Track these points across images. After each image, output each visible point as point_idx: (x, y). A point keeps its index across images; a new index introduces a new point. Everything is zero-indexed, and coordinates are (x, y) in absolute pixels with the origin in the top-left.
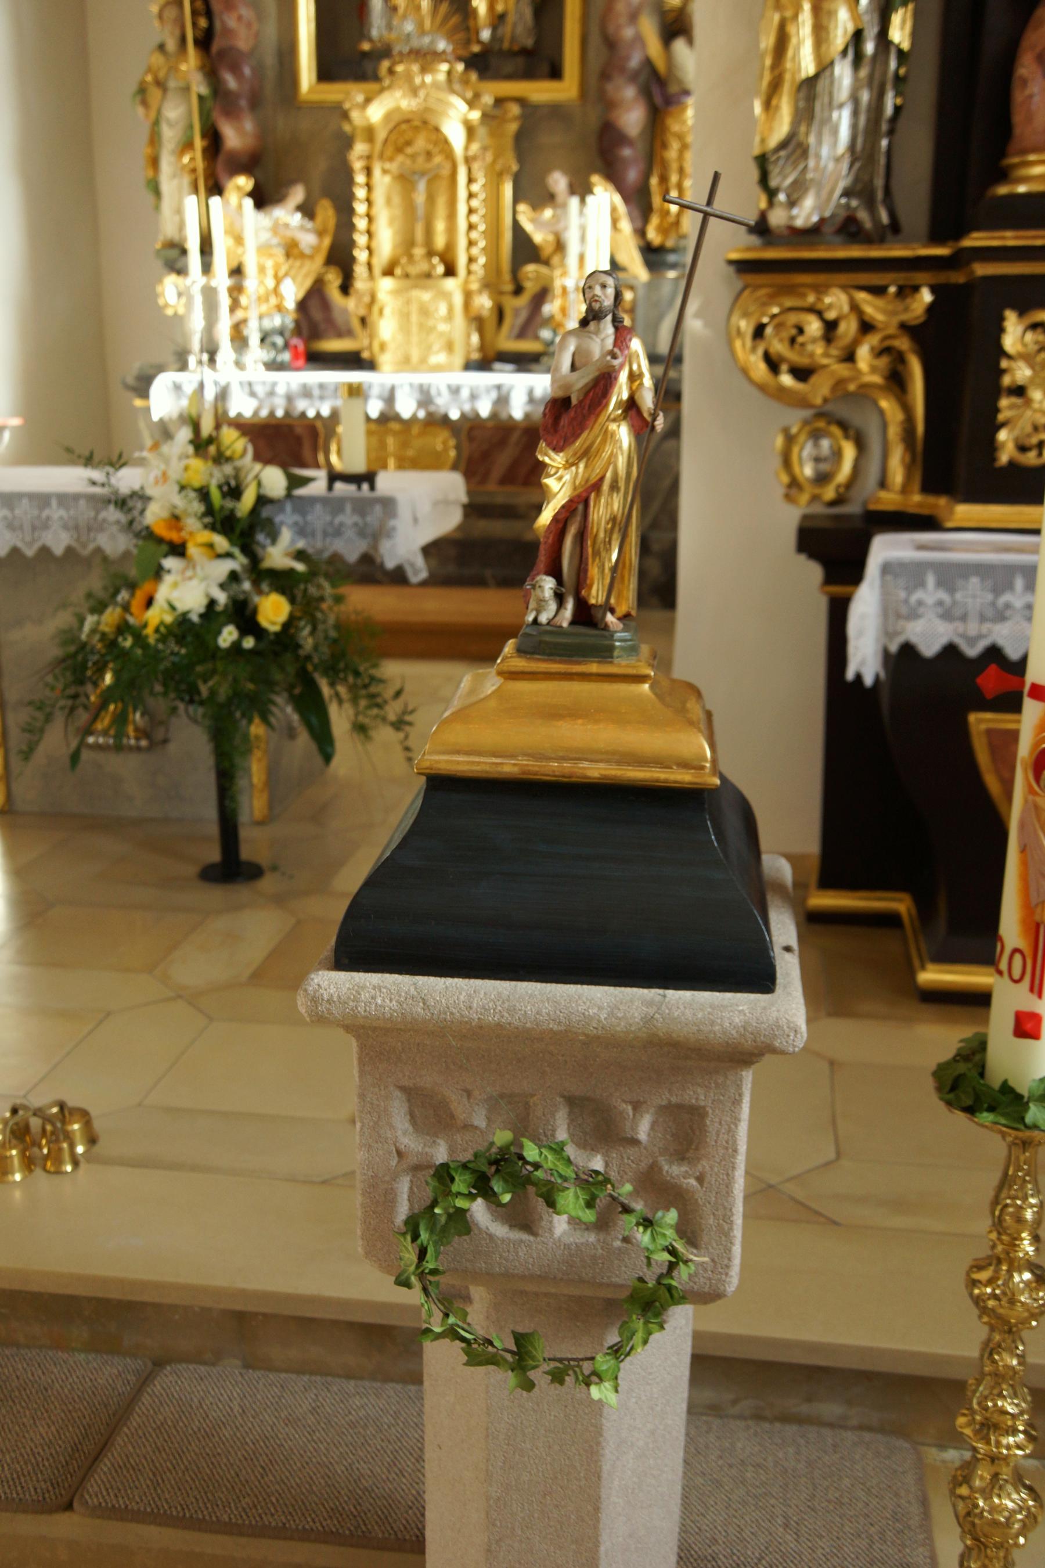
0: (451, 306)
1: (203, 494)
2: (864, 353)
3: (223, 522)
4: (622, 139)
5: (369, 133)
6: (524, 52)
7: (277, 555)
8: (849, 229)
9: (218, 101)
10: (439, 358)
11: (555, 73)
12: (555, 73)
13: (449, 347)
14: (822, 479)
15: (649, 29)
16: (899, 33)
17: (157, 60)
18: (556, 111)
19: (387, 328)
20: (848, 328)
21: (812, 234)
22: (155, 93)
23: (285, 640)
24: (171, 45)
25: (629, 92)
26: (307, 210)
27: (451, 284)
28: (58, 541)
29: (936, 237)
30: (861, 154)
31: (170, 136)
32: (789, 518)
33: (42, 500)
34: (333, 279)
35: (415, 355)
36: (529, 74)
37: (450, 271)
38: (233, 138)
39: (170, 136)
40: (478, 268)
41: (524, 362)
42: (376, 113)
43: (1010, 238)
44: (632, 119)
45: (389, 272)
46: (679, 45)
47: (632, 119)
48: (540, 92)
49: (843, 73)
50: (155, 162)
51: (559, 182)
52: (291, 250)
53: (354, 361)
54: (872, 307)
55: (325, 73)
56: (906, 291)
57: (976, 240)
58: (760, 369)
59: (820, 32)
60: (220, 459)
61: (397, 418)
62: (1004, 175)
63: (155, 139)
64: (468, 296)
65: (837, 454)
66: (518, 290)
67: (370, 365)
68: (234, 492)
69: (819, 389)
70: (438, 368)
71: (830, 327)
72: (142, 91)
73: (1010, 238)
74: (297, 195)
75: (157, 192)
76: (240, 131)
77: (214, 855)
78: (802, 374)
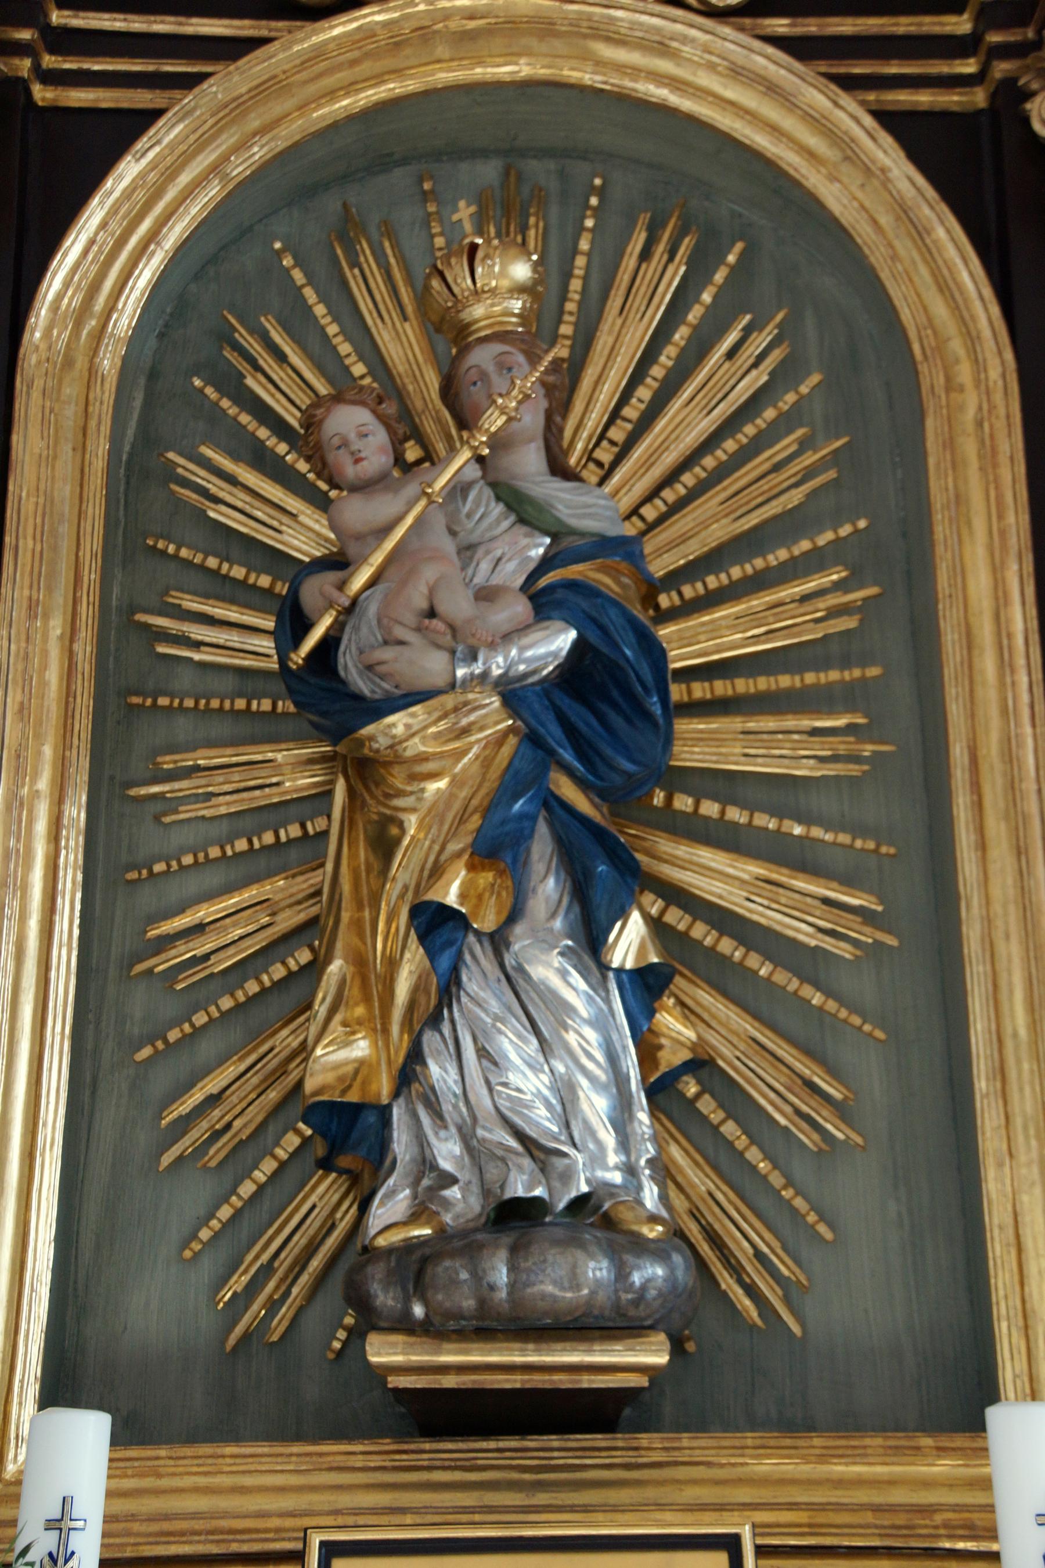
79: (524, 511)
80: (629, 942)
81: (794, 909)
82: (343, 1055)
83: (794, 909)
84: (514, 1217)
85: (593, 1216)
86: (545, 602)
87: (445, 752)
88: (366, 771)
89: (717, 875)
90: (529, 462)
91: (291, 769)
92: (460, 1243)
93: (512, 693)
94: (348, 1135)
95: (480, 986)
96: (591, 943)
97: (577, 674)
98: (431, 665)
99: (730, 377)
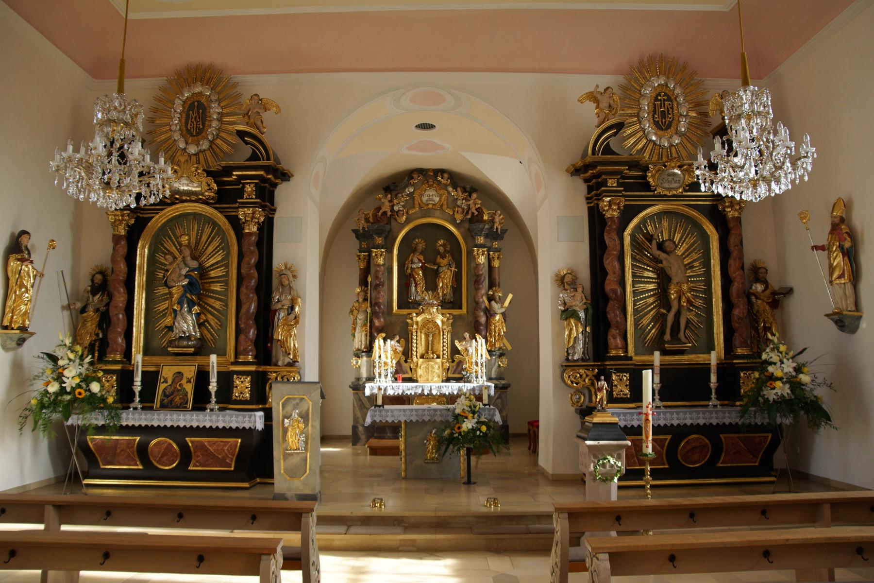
0: (437, 366)
1: (470, 407)
2: (587, 380)
3: (474, 413)
4: (481, 324)
5: (417, 323)
6: (451, 302)
7: (483, 419)
8: (583, 360)
9: (374, 314)
10: (436, 379)
11: (461, 308)
12: (461, 308)
13: (439, 376)
14: (578, 402)
15: (485, 299)
16: (588, 329)
17: (357, 305)
18: (460, 316)
19: (420, 372)
20: (584, 376)
21: (577, 361)
22: (355, 312)
23: (485, 434)
24: (361, 300)
25: (482, 314)
26: (398, 342)
27: (438, 360)
28: (427, 418)
29: (595, 361)
30: (584, 348)
31: (360, 322)
32: (573, 409)
33: (424, 410)
34: (403, 358)
35: (430, 379)
36: (453, 308)
37: (438, 357)
38: (377, 323)
39: (360, 322)
40: (445, 356)
41: (458, 380)
42: (419, 319)
43: (612, 363)
44: (483, 320)
45: (422, 357)
46: (493, 303)
47: (483, 320)
48: (456, 312)
49: (580, 335)
50: (355, 329)
51: (467, 335)
52: (395, 351)
53: (410, 380)
54: (588, 373)
55: (399, 307)
56: (593, 370)
57: (607, 363)
58: (569, 382)
59: (577, 330)
60: (470, 401)
61: (432, 394)
62: (608, 352)
63: (355, 323)
64: (443, 363)
65: (580, 398)
66: (453, 361)
67: (416, 381)
68: (475, 407)
69: (580, 386)
70: (435, 382)
71: (581, 376)
72: (352, 311)
73: (612, 363)
74: (397, 338)
75: (354, 336)
76: (380, 321)
77: (465, 480)
78: (577, 384)
79: (186, 265)
80: (196, 308)
81: (217, 305)
82: (168, 321)
83: (217, 305)
84: (181, 337)
85: (189, 338)
86: (186, 276)
87: (177, 292)
88: (170, 293)
89: (211, 301)
90: (189, 258)
91: (166, 291)
92: (175, 340)
93: (183, 286)
94: (170, 328)
95: (179, 318)
96: (190, 311)
97: (190, 284)
98: (174, 284)
99: (215, 243)
